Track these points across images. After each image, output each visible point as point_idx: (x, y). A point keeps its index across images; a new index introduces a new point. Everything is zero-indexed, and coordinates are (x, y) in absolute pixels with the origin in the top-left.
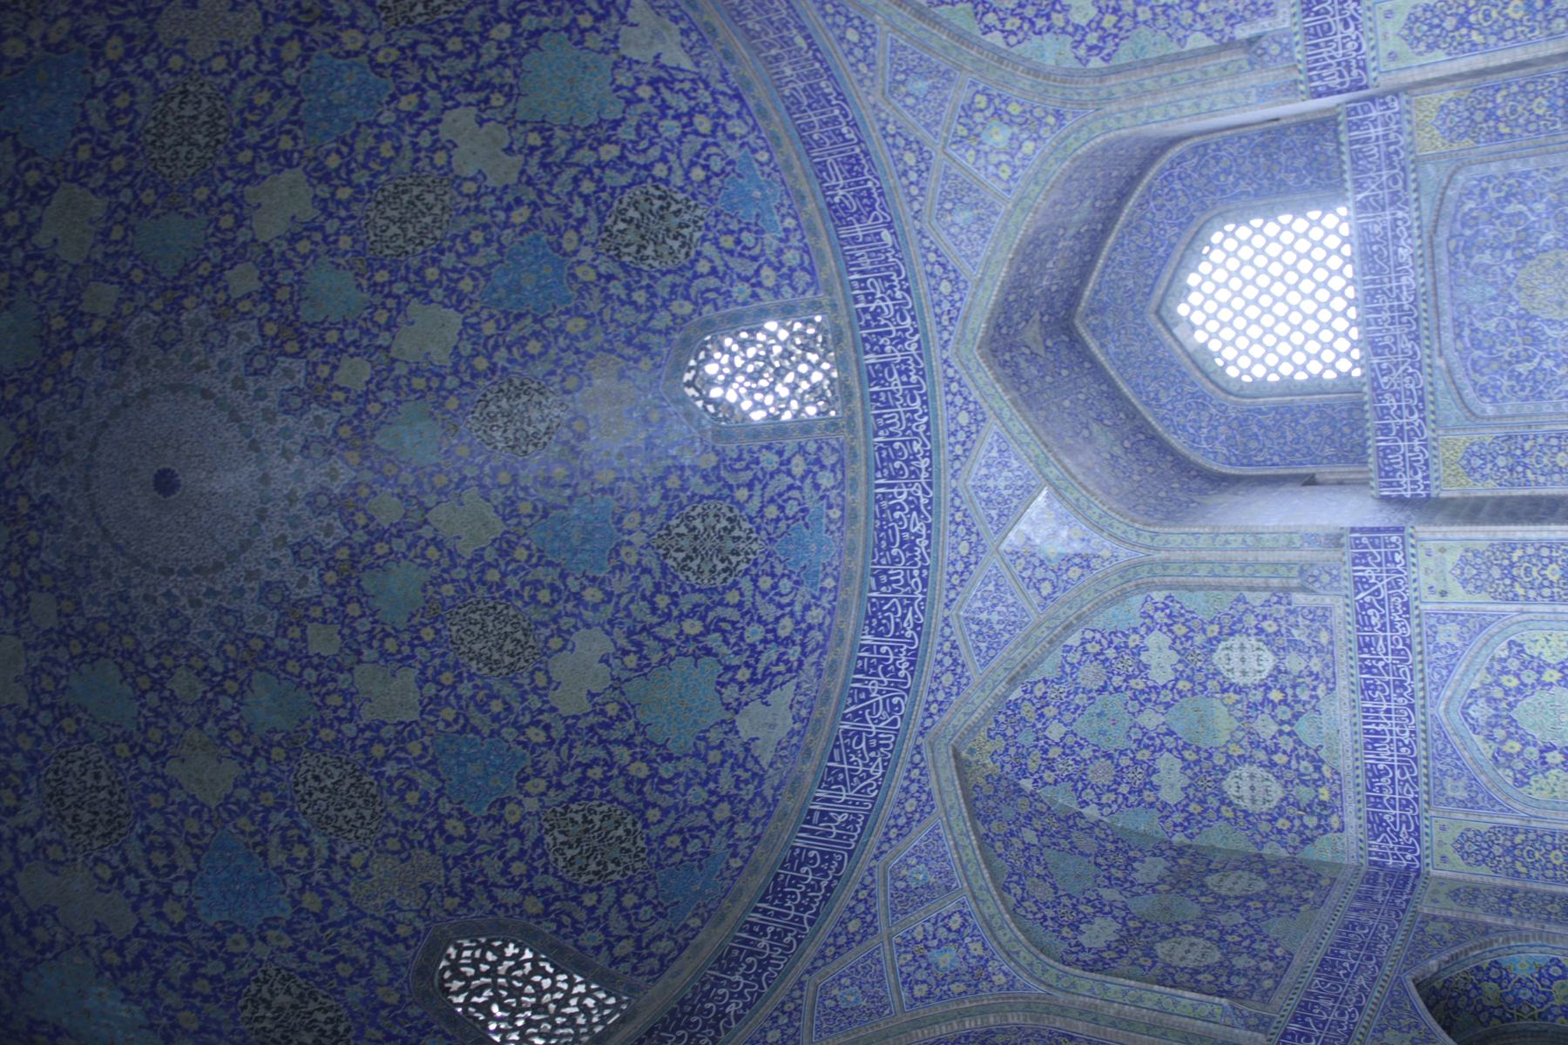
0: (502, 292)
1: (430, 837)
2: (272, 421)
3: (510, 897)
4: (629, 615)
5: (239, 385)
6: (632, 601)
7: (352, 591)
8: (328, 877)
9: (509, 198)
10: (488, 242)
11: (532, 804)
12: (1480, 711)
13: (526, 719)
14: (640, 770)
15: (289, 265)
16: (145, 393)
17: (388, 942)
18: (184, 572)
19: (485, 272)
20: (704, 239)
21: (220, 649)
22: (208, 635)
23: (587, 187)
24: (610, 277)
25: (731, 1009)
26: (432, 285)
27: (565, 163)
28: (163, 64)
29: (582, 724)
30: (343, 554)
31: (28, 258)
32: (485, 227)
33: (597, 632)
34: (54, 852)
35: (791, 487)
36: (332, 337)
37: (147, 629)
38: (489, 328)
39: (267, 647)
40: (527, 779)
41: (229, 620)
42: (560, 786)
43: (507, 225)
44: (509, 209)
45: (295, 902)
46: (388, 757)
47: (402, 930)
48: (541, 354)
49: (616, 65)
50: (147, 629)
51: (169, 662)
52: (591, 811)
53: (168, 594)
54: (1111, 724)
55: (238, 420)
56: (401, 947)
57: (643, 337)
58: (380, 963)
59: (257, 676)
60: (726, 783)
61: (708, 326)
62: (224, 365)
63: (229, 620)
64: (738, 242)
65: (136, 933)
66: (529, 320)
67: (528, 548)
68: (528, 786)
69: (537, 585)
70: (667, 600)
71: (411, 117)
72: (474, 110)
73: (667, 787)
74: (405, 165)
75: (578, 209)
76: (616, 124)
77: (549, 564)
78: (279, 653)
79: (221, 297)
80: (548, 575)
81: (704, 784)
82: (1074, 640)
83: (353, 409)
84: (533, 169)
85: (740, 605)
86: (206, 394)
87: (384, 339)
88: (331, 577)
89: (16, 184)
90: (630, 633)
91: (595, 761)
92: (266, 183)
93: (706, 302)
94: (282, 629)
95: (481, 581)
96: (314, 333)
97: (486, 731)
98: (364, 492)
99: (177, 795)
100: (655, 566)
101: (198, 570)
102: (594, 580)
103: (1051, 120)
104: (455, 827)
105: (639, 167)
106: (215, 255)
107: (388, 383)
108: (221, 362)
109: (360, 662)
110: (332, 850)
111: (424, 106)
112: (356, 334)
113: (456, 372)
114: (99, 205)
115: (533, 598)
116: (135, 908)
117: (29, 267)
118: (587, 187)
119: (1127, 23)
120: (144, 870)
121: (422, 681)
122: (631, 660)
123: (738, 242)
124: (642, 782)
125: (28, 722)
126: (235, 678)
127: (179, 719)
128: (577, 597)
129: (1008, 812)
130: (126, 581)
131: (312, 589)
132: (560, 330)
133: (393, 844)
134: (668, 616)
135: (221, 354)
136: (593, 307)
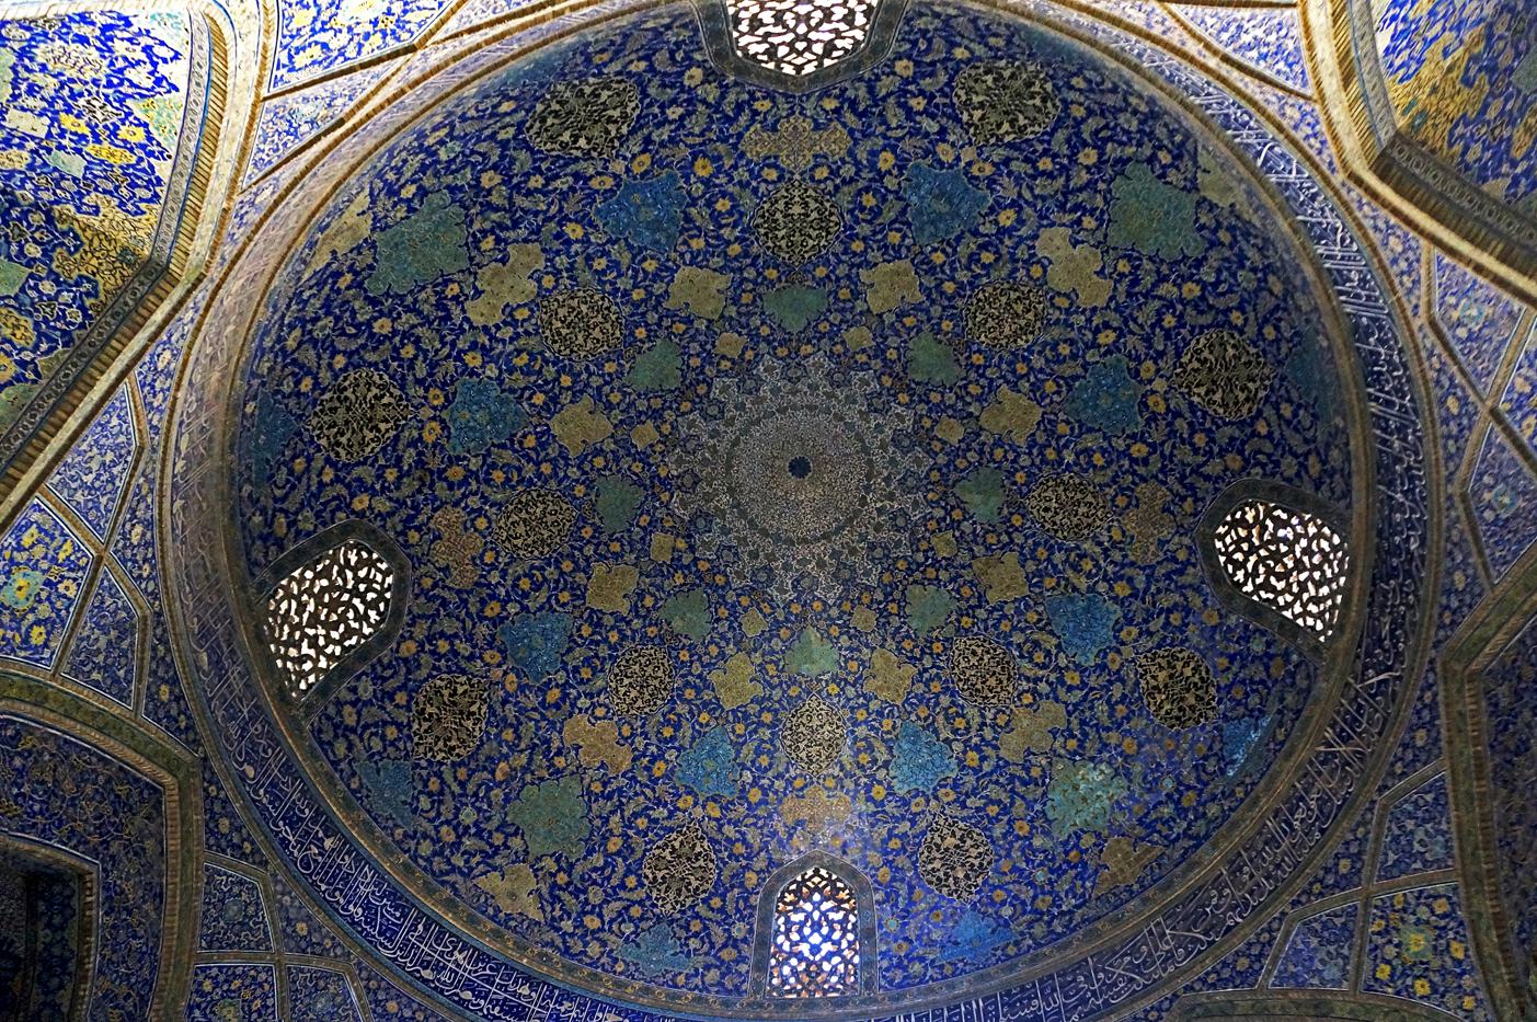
1: (1134, 473)
4: (1044, 198)
5: (730, 422)
6: (1031, 189)
11: (1160, 385)
13: (1090, 336)
14: (1191, 290)
16: (731, 491)
17: (1181, 572)
29: (1121, 298)
31: (637, 616)
33: (1045, 234)
40: (1138, 372)
42: (1161, 354)
45: (1115, 599)
47: (1182, 556)
52: (1198, 352)
56: (1191, 570)
58: (1189, 593)
65: (1069, 714)
67: (935, 250)
68: (1144, 375)
69: (973, 258)
70: (1048, 160)
73: (1223, 288)
77: (959, 239)
80: (969, 246)
83: (763, 345)
86: (735, 443)
90: (1062, 207)
95: (950, 299)
98: (839, 348)
99: (1009, 610)
102: (992, 210)
104: (1139, 450)
110: (1100, 544)
114: (599, 569)
115: (984, 266)
116: (1057, 700)
117: (643, 612)
122: (1089, 223)
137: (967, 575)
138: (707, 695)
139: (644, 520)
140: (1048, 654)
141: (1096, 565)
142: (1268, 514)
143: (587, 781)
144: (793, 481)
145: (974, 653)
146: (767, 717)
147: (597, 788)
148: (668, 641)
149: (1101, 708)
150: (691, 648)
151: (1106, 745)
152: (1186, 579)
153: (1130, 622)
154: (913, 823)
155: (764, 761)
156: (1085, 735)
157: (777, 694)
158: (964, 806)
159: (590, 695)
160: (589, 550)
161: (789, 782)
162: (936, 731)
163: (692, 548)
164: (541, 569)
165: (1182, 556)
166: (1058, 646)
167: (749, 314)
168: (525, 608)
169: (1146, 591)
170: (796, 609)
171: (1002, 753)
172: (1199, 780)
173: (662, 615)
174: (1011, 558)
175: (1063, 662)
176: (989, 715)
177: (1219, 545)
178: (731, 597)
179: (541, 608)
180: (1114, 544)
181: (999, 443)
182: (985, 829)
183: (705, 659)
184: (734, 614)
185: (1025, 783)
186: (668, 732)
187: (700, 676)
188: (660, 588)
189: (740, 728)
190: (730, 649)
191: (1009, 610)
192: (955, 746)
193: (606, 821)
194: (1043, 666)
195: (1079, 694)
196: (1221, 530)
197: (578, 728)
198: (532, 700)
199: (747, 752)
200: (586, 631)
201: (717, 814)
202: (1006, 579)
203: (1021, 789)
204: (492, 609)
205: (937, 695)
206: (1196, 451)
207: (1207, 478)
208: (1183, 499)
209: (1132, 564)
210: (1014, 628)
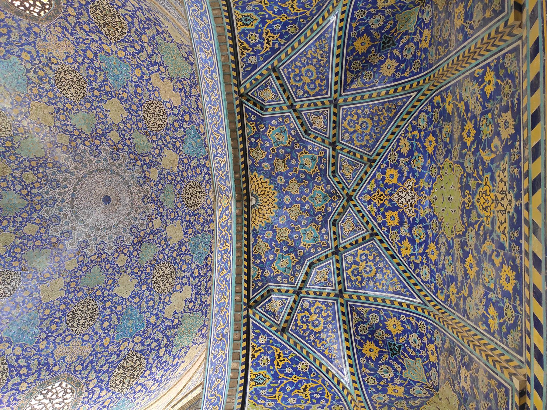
0: (130, 312)
2: (116, 234)
7: (45, 245)
16: (132, 193)
18: (73, 195)
19: (139, 307)
21: (40, 194)
22: (47, 193)
26: (141, 288)
31: (161, 146)
32: (153, 306)
36: (135, 254)
37: (54, 174)
38: (119, 308)
39: (36, 210)
41: (51, 202)
48: (102, 327)
50: (54, 174)
51: (40, 175)
53: (66, 186)
55: (119, 223)
59: (26, 203)
63: (51, 202)
66: (116, 323)
78: (32, 213)
79: (154, 217)
89: (175, 139)
93: (89, 394)
96: (138, 248)
98: (80, 259)
101: (73, 200)
107: (114, 272)
108: (136, 218)
109: (16, 237)
112: (133, 262)
113: (109, 295)
114: (175, 170)
117: (159, 147)
126: (27, 195)
127: (17, 169)
131: (52, 232)
132: (108, 335)
135: (139, 218)
139: (160, 187)
144: (109, 194)
146: (97, 93)
148: (147, 132)
150: (138, 128)
160: (178, 179)
161: (75, 61)
163: (144, 171)
168: (198, 160)
179: (193, 158)
186: (139, 90)
187: (132, 115)
188: (153, 156)
190: (122, 125)
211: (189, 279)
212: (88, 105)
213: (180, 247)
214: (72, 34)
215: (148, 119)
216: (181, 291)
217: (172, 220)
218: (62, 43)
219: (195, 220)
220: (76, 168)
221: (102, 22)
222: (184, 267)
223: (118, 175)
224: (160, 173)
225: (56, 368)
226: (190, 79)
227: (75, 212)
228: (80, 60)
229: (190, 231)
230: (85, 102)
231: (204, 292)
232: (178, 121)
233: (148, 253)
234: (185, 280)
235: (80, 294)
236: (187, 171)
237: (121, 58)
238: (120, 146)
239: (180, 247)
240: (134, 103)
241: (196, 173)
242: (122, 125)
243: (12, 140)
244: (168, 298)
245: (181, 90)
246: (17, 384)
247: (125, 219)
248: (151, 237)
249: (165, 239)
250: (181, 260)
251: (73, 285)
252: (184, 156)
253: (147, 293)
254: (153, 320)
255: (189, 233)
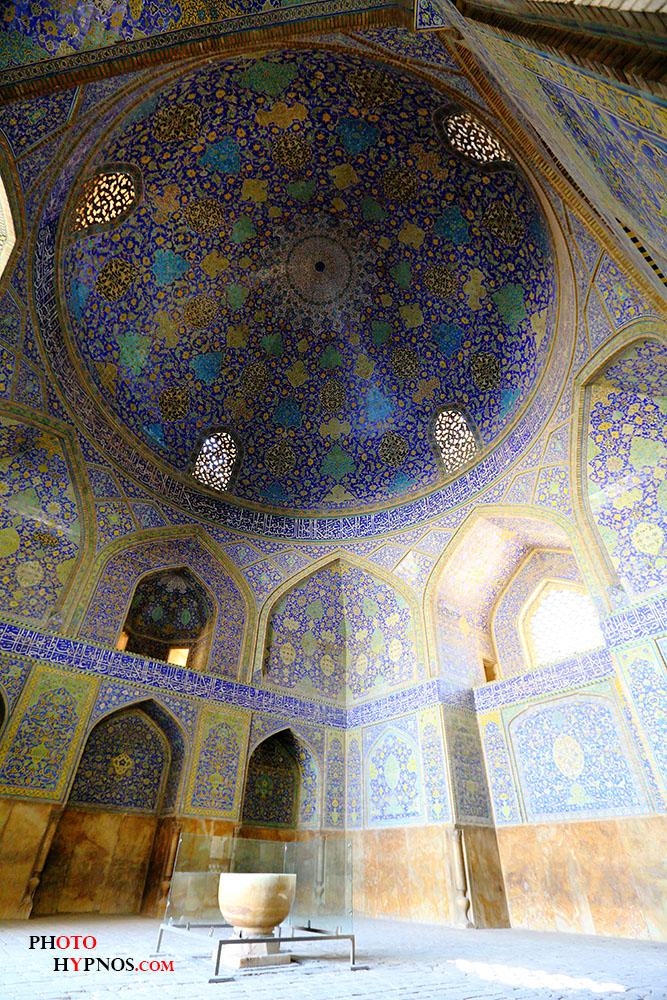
1: (259, 411)
3: (251, 442)
8: (228, 390)
9: (467, 312)
10: (450, 316)
12: (391, 742)
14: (311, 462)
15: (400, 254)
16: (334, 240)
17: (217, 415)
18: (296, 292)
19: (441, 321)
20: (490, 392)
23: (486, 338)
24: (463, 366)
25: (228, 520)
26: (426, 306)
27: (489, 324)
28: (405, 159)
30: (333, 335)
31: (322, 173)
32: (454, 311)
34: (176, 315)
35: (420, 468)
36: (392, 285)
37: (269, 294)
42: (295, 440)
43: (459, 318)
44: (464, 315)
45: (213, 385)
46: (277, 386)
47: (223, 418)
49: (526, 319)
50: (269, 294)
51: (263, 307)
52: (291, 454)
53: (285, 292)
54: (371, 610)
57: (451, 390)
58: (209, 417)
59: (278, 334)
60: (315, 490)
61: (464, 411)
62: (361, 258)
64: (494, 406)
65: (171, 350)
68: (290, 431)
71: (467, 257)
72: (484, 278)
74: (453, 268)
75: (478, 340)
76: (510, 334)
79: (375, 240)
81: (312, 484)
82: (389, 588)
84: (481, 314)
85: (376, 469)
87: (402, 302)
88: (324, 336)
89: (331, 151)
91: (308, 447)
92: (413, 226)
93: (471, 406)
94: (298, 331)
96: (388, 279)
97: (301, 410)
98: (356, 329)
99: (223, 335)
100: (380, 435)
103: (567, 509)
104: (266, 416)
105: (502, 353)
106: (383, 228)
111: (473, 259)
113: (407, 333)
114: (357, 180)
116: (178, 345)
117: (321, 176)
118: (486, 338)
119: (619, 525)
120: (192, 340)
121: (307, 382)
122: (346, 443)
123: (494, 406)
124: (306, 465)
125: (208, 283)
128: (359, 416)
129: (327, 583)
130: (279, 278)
131: (317, 333)
132: (439, 360)
133: (250, 402)
134: (365, 448)
135: (362, 254)
136: (452, 367)
137: (244, 321)
138: (260, 175)
139: (356, 209)
140: (199, 347)
141: (229, 382)
142: (232, 458)
143: (269, 98)
144: (317, 260)
145: (210, 311)
146: (228, 196)
147: (260, 100)
148: (298, 175)
149: (170, 366)
151: (154, 365)
152: (214, 417)
153: (203, 388)
154: (137, 257)
155: (207, 186)
156: (160, 356)
157: (236, 206)
158: (139, 286)
159: (309, 130)
160: (368, 185)
161: (188, 194)
162: (180, 279)
163: (327, 212)
164: (382, 167)
165: (223, 418)
166: (201, 353)
167: (391, 318)
168: (376, 147)
169: (214, 399)
170: (268, 233)
171: (160, 312)
172: (141, 411)
173: (312, 182)
174: (244, 345)
175: (194, 353)
176: (179, 310)
177: (224, 434)
178: (294, 210)
179: (368, 151)
180: (235, 392)
181: (290, 363)
182: (126, 297)
183: (276, 184)
184: (285, 206)
185: (144, 320)
186: (257, 147)
188: (323, 189)
189: (231, 181)
190: (272, 196)
191: (223, 335)
192: (170, 288)
193: (237, 95)
194: (194, 342)
195: (178, 356)
196: (229, 437)
197: (300, 113)
198: (334, 109)
199: (217, 179)
200: (338, 153)
201: (194, 150)
202: (236, 339)
203: (141, 318)
204: (391, 139)
205: (197, 285)
206: (259, 437)
207: (248, 438)
208: (243, 426)
209: (225, 396)
210: (214, 334)
211: (467, 264)
212: (232, 215)
213: (430, 244)
214: (164, 177)
215: (288, 163)
216: (468, 278)
217: (397, 227)
218: (166, 194)
219: (424, 207)
220: (275, 271)
221: (173, 133)
222: (452, 257)
223: (307, 238)
224: (344, 198)
225: (427, 409)
226: (300, 76)
227: (312, 302)
228: (189, 188)
229: (427, 221)
230: (228, 216)
231: (496, 263)
232: (319, 132)
233: (403, 275)
234: (464, 268)
235: (385, 352)
236: (371, 169)
237: (216, 141)
238: (287, 214)
239: (430, 244)
240: (263, 165)
241: (384, 162)
242: (272, 196)
243: (222, 306)
244: (461, 295)
245: (297, 98)
246: (415, 437)
247: (351, 265)
248: (391, 259)
249: (407, 249)
250: (443, 254)
251: (373, 351)
252: (355, 157)
253: (437, 306)
254: (465, 321)
255: (428, 223)
